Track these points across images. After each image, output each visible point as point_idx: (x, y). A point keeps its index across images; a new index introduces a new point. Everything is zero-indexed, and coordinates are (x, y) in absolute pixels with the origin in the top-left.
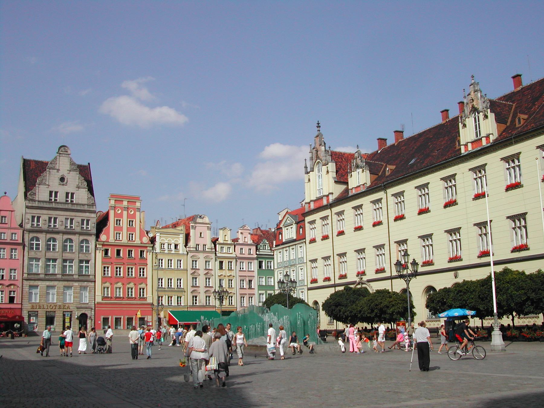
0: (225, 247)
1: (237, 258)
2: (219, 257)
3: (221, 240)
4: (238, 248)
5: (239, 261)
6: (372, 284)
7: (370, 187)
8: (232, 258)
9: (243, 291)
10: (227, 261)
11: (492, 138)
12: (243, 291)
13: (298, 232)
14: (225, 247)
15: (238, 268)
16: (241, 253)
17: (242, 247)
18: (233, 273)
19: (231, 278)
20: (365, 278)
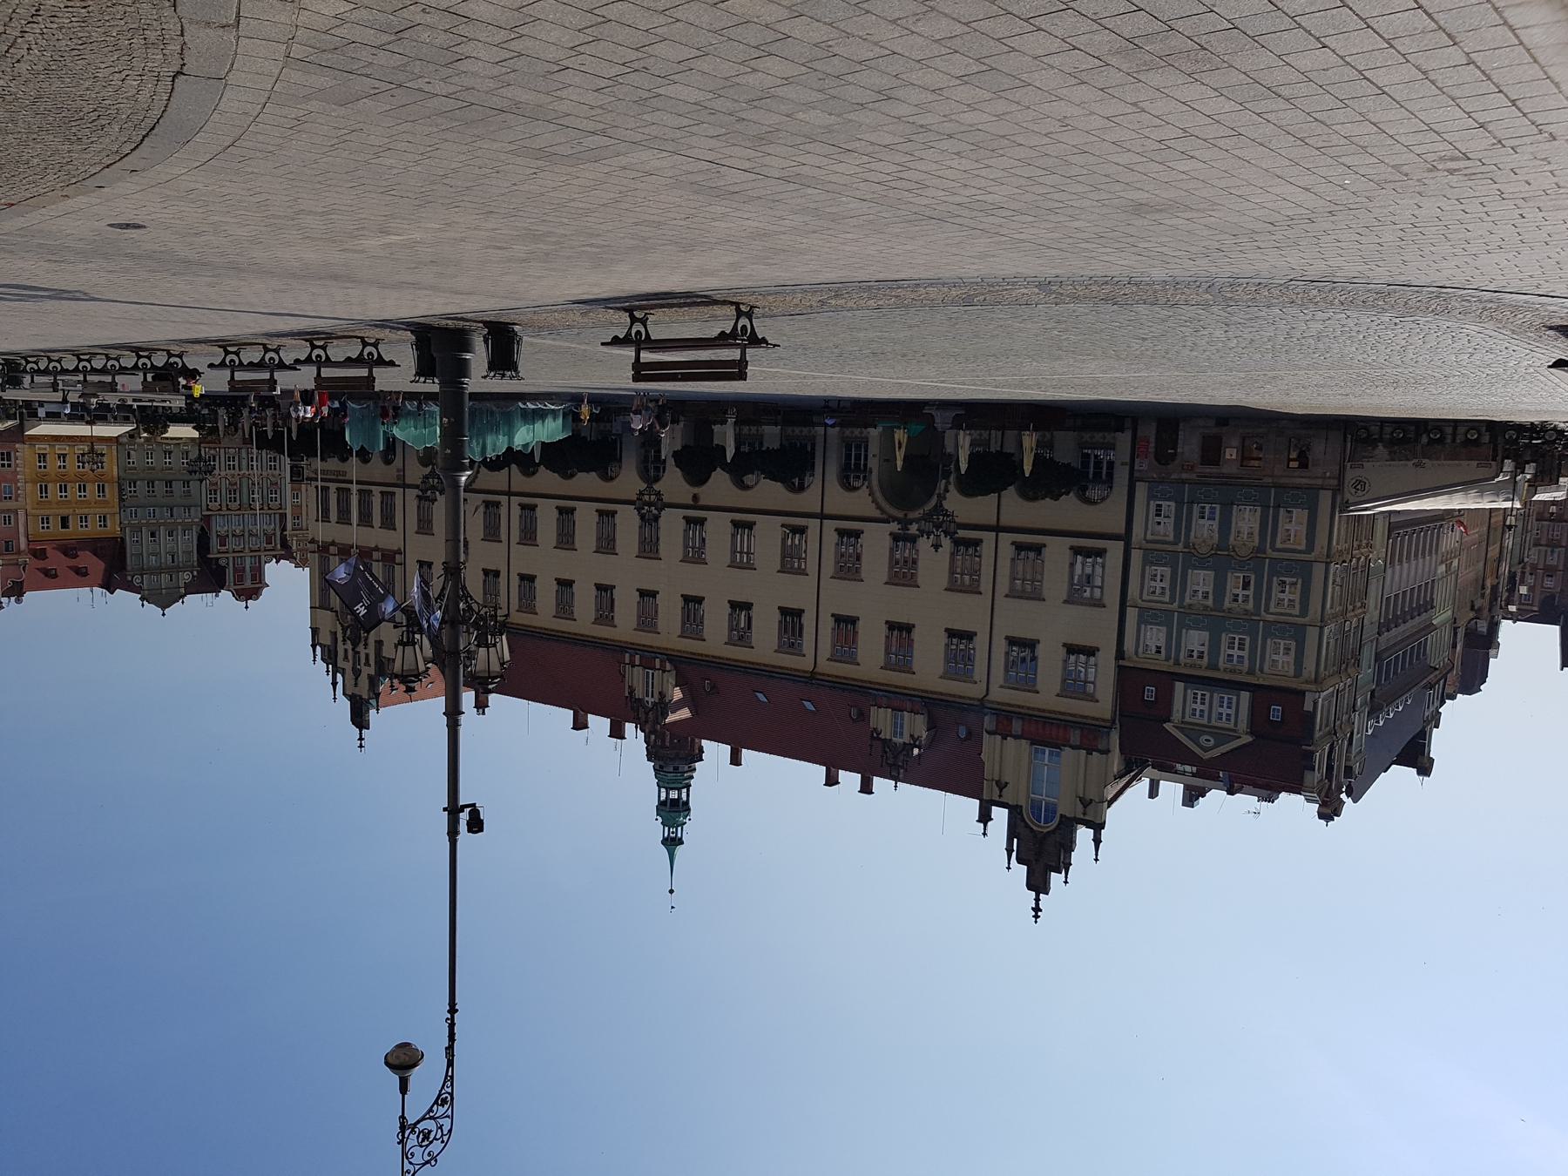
6: (877, 514)
20: (894, 527)
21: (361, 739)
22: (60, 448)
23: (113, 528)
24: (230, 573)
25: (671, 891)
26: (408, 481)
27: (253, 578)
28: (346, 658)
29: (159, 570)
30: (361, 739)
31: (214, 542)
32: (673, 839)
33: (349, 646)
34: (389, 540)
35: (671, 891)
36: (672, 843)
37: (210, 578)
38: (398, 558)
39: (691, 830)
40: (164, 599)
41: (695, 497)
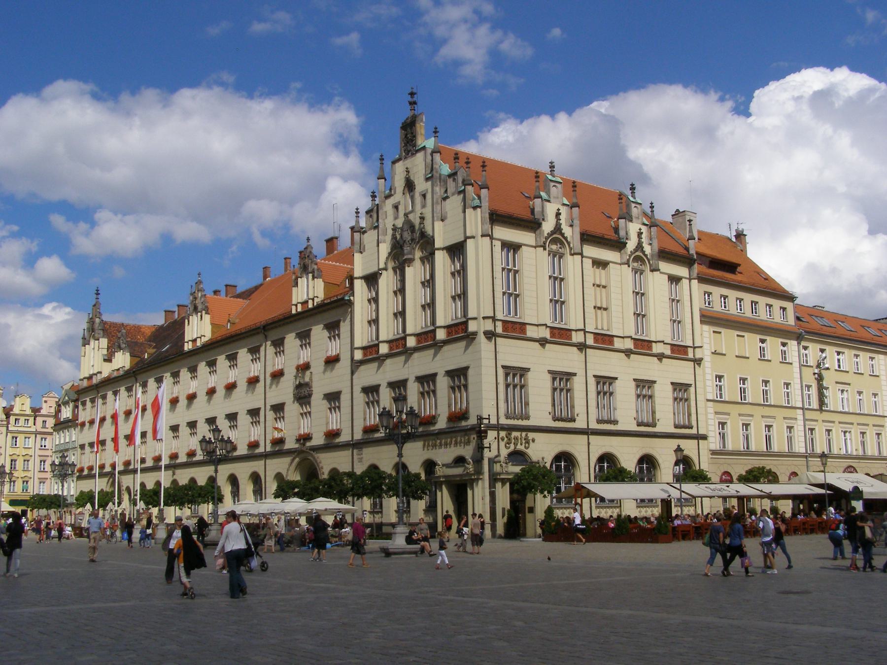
0: (22, 419)
1: (36, 433)
2: (12, 432)
3: (16, 410)
4: (39, 420)
5: (39, 437)
7: (128, 370)
8: (31, 433)
9: (43, 475)
10: (23, 436)
11: (204, 340)
12: (43, 475)
13: (74, 411)
14: (22, 419)
15: (38, 446)
16: (44, 427)
17: (45, 419)
18: (31, 452)
19: (27, 458)
21: (413, 103)
30: (413, 103)
38: (359, 355)
41: (174, 474)
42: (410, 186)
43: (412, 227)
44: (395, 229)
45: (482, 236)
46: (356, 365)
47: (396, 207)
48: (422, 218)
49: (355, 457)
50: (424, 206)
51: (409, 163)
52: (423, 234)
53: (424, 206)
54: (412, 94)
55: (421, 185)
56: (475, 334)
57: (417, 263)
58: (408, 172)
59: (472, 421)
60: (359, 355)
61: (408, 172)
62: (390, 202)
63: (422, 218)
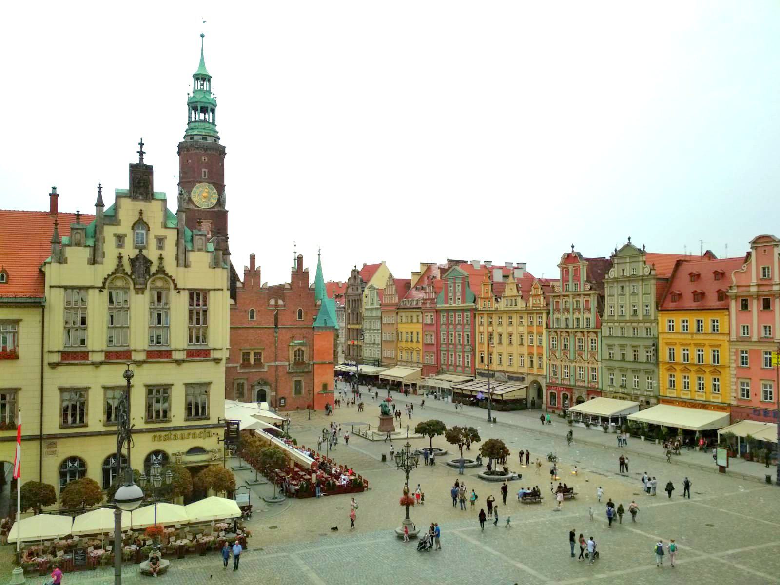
21: (141, 153)
22: (701, 397)
23: (664, 320)
24: (584, 274)
25: (202, 36)
26: (35, 444)
27: (567, 271)
28: (161, 241)
29: (633, 279)
30: (141, 153)
31: (593, 303)
32: (204, 80)
33: (152, 254)
34: (74, 376)
35: (202, 36)
36: (202, 78)
37: (599, 269)
39: (187, 88)
40: (629, 252)
42: (140, 223)
43: (148, 262)
44: (120, 258)
45: (228, 290)
46: (48, 366)
47: (120, 238)
48: (161, 259)
49: (45, 450)
50: (161, 248)
51: (141, 205)
52: (161, 270)
53: (161, 248)
54: (141, 145)
55: (156, 230)
56: (221, 360)
57: (147, 292)
58: (141, 213)
59: (214, 420)
60: (56, 358)
61: (141, 213)
62: (109, 231)
63: (161, 259)
